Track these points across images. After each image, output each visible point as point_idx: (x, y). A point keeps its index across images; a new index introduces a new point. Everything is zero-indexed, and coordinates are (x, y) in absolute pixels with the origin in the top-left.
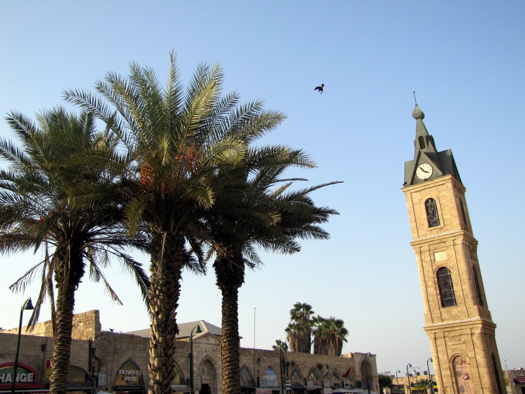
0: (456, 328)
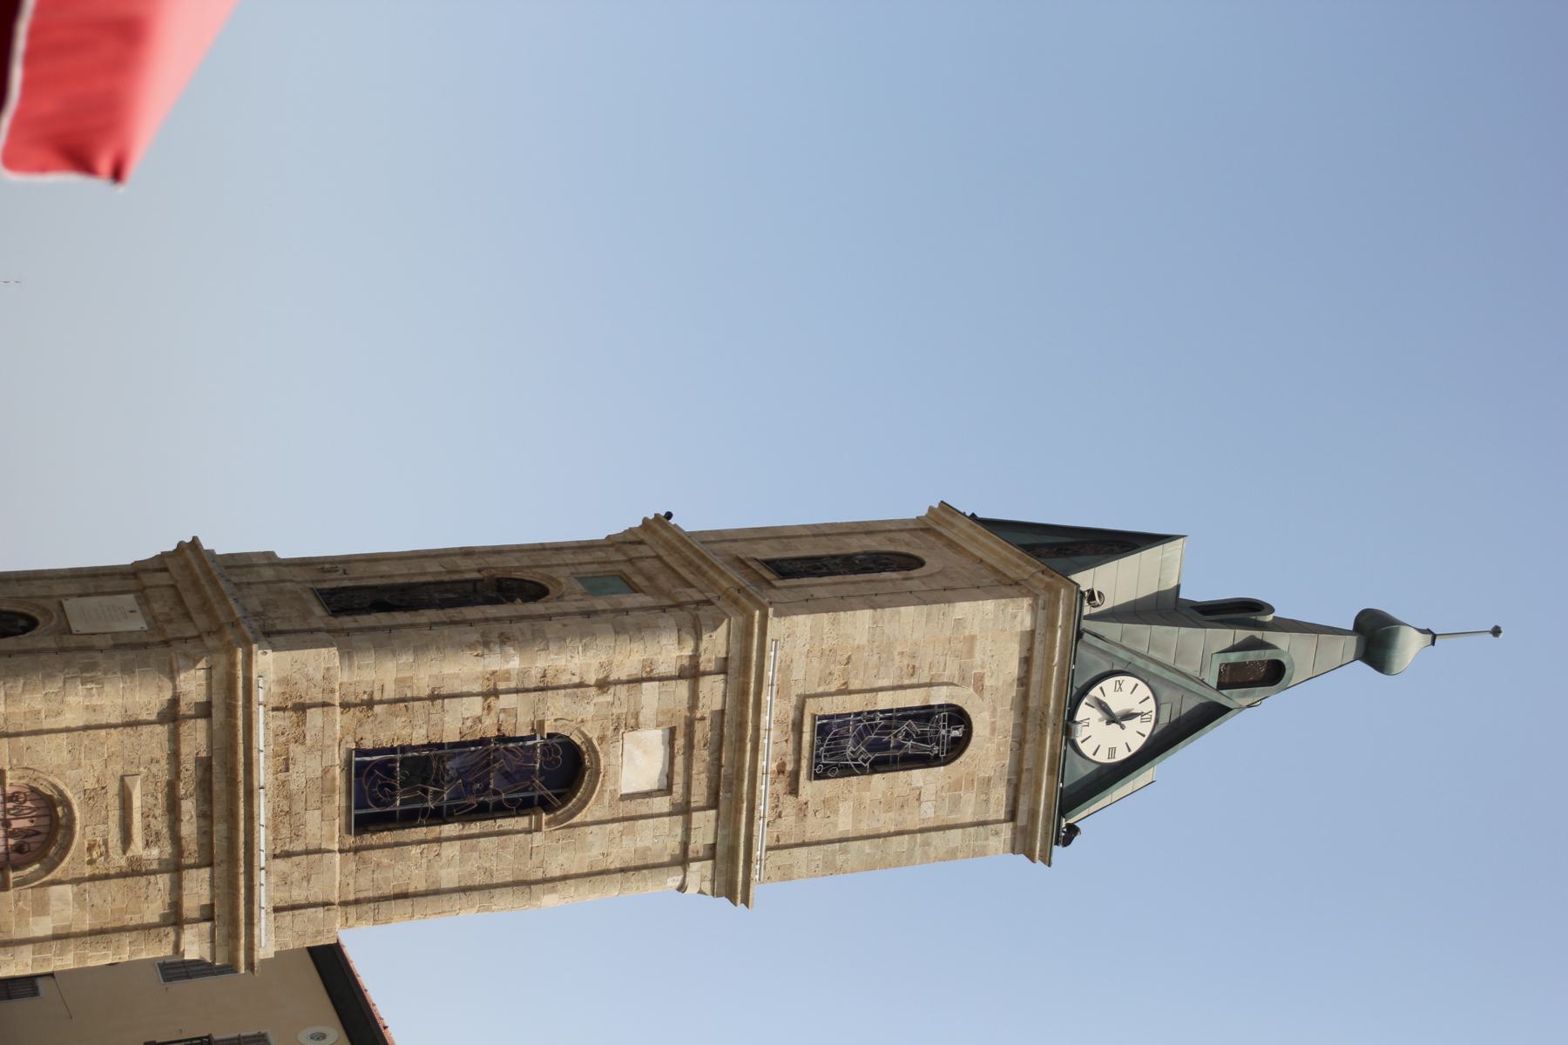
0: (220, 829)
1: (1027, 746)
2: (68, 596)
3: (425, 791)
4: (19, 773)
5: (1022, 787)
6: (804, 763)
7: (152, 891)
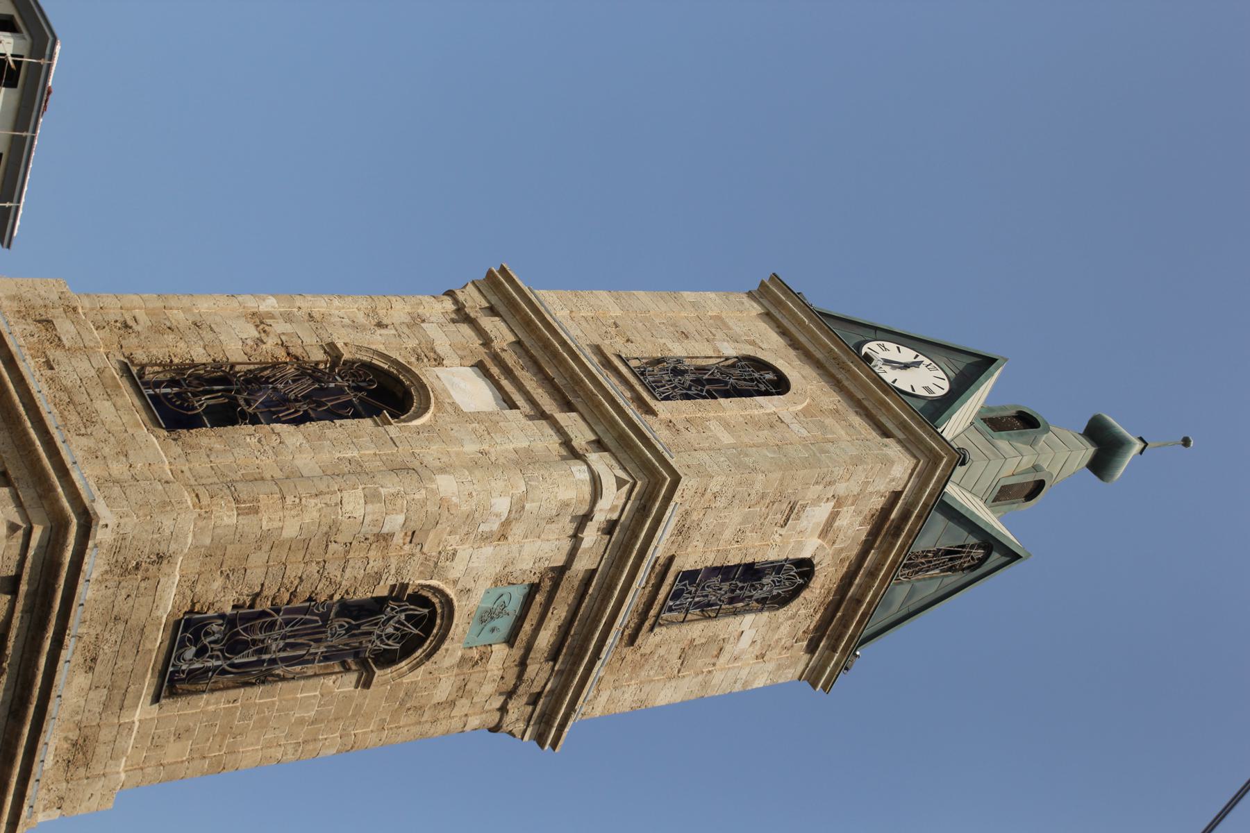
1: (846, 383)
3: (236, 399)
5: (874, 412)
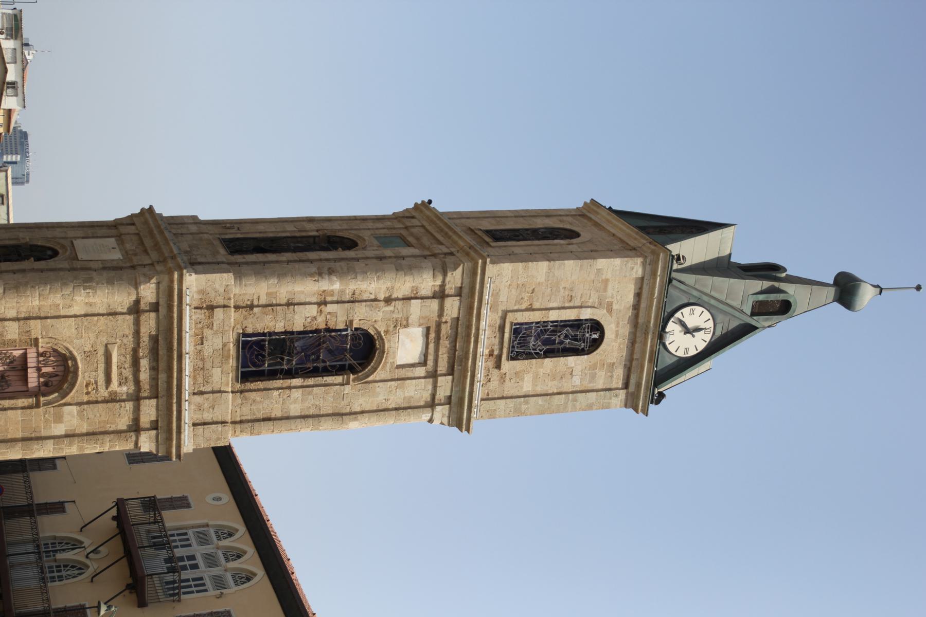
0: (162, 377)
1: (637, 345)
2: (76, 238)
3: (282, 359)
4: (47, 340)
5: (633, 369)
6: (505, 351)
7: (123, 411)
